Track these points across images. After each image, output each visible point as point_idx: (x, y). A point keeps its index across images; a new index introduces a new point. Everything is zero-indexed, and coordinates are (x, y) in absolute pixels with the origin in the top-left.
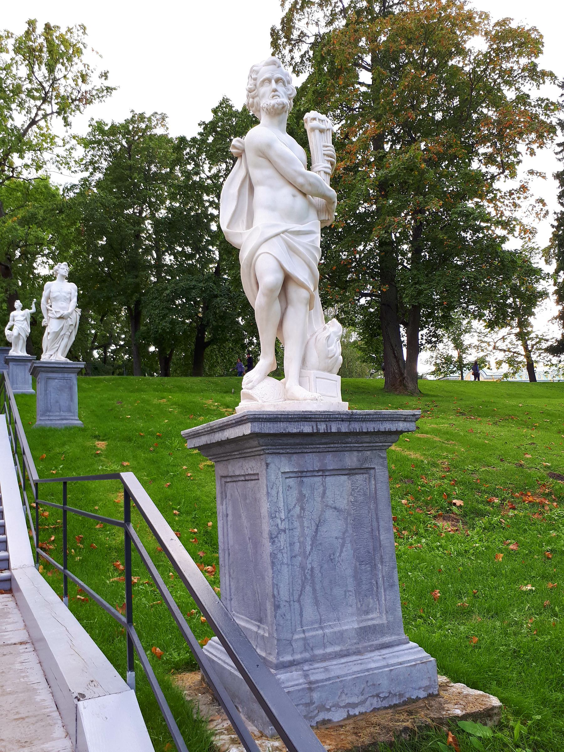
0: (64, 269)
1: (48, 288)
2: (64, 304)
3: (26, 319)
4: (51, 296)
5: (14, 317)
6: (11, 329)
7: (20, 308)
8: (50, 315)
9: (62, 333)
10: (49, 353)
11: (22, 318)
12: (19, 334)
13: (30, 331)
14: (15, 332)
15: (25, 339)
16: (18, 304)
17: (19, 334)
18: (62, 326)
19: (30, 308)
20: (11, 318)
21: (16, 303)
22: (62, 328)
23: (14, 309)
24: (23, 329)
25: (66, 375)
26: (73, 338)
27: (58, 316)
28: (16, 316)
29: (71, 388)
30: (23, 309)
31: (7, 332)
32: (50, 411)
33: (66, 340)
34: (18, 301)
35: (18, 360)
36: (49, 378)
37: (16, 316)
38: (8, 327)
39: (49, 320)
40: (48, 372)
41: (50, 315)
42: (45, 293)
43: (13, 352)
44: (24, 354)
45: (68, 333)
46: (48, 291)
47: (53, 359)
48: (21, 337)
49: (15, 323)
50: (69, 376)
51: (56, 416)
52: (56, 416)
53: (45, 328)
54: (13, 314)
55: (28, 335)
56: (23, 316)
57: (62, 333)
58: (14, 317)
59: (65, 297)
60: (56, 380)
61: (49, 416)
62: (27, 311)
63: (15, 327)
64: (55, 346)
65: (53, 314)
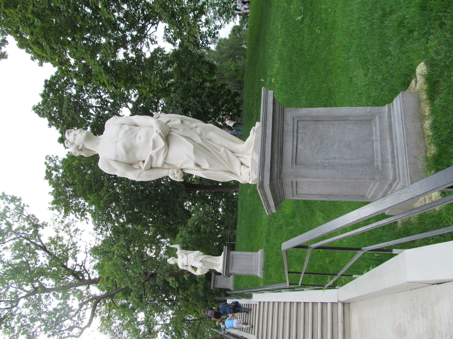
0: (75, 135)
1: (110, 165)
2: (141, 133)
3: (186, 254)
4: (125, 159)
5: (183, 265)
6: (194, 268)
7: (176, 259)
8: (159, 162)
9: (198, 140)
10: (237, 168)
11: (185, 257)
12: (201, 261)
13: (198, 252)
14: (198, 264)
15: (206, 256)
17: (201, 261)
18: (184, 140)
19: (177, 250)
20: (185, 268)
21: (170, 263)
22: (188, 138)
23: (176, 265)
24: (195, 257)
25: (289, 127)
27: (161, 143)
28: (183, 263)
29: (317, 120)
30: (177, 257)
32: (373, 161)
33: (212, 135)
35: (227, 264)
36: (295, 160)
37: (183, 263)
38: (193, 272)
39: (171, 166)
40: (281, 163)
41: (159, 162)
42: (120, 172)
43: (219, 269)
46: (114, 165)
48: (204, 260)
49: (190, 265)
50: (290, 122)
51: (383, 148)
52: (383, 148)
53: (187, 176)
55: (202, 253)
56: (183, 257)
57: (198, 140)
58: (183, 265)
59: (126, 132)
60: (300, 147)
61: (384, 162)
62: (179, 252)
63: (193, 265)
64: (224, 155)
65: (158, 154)
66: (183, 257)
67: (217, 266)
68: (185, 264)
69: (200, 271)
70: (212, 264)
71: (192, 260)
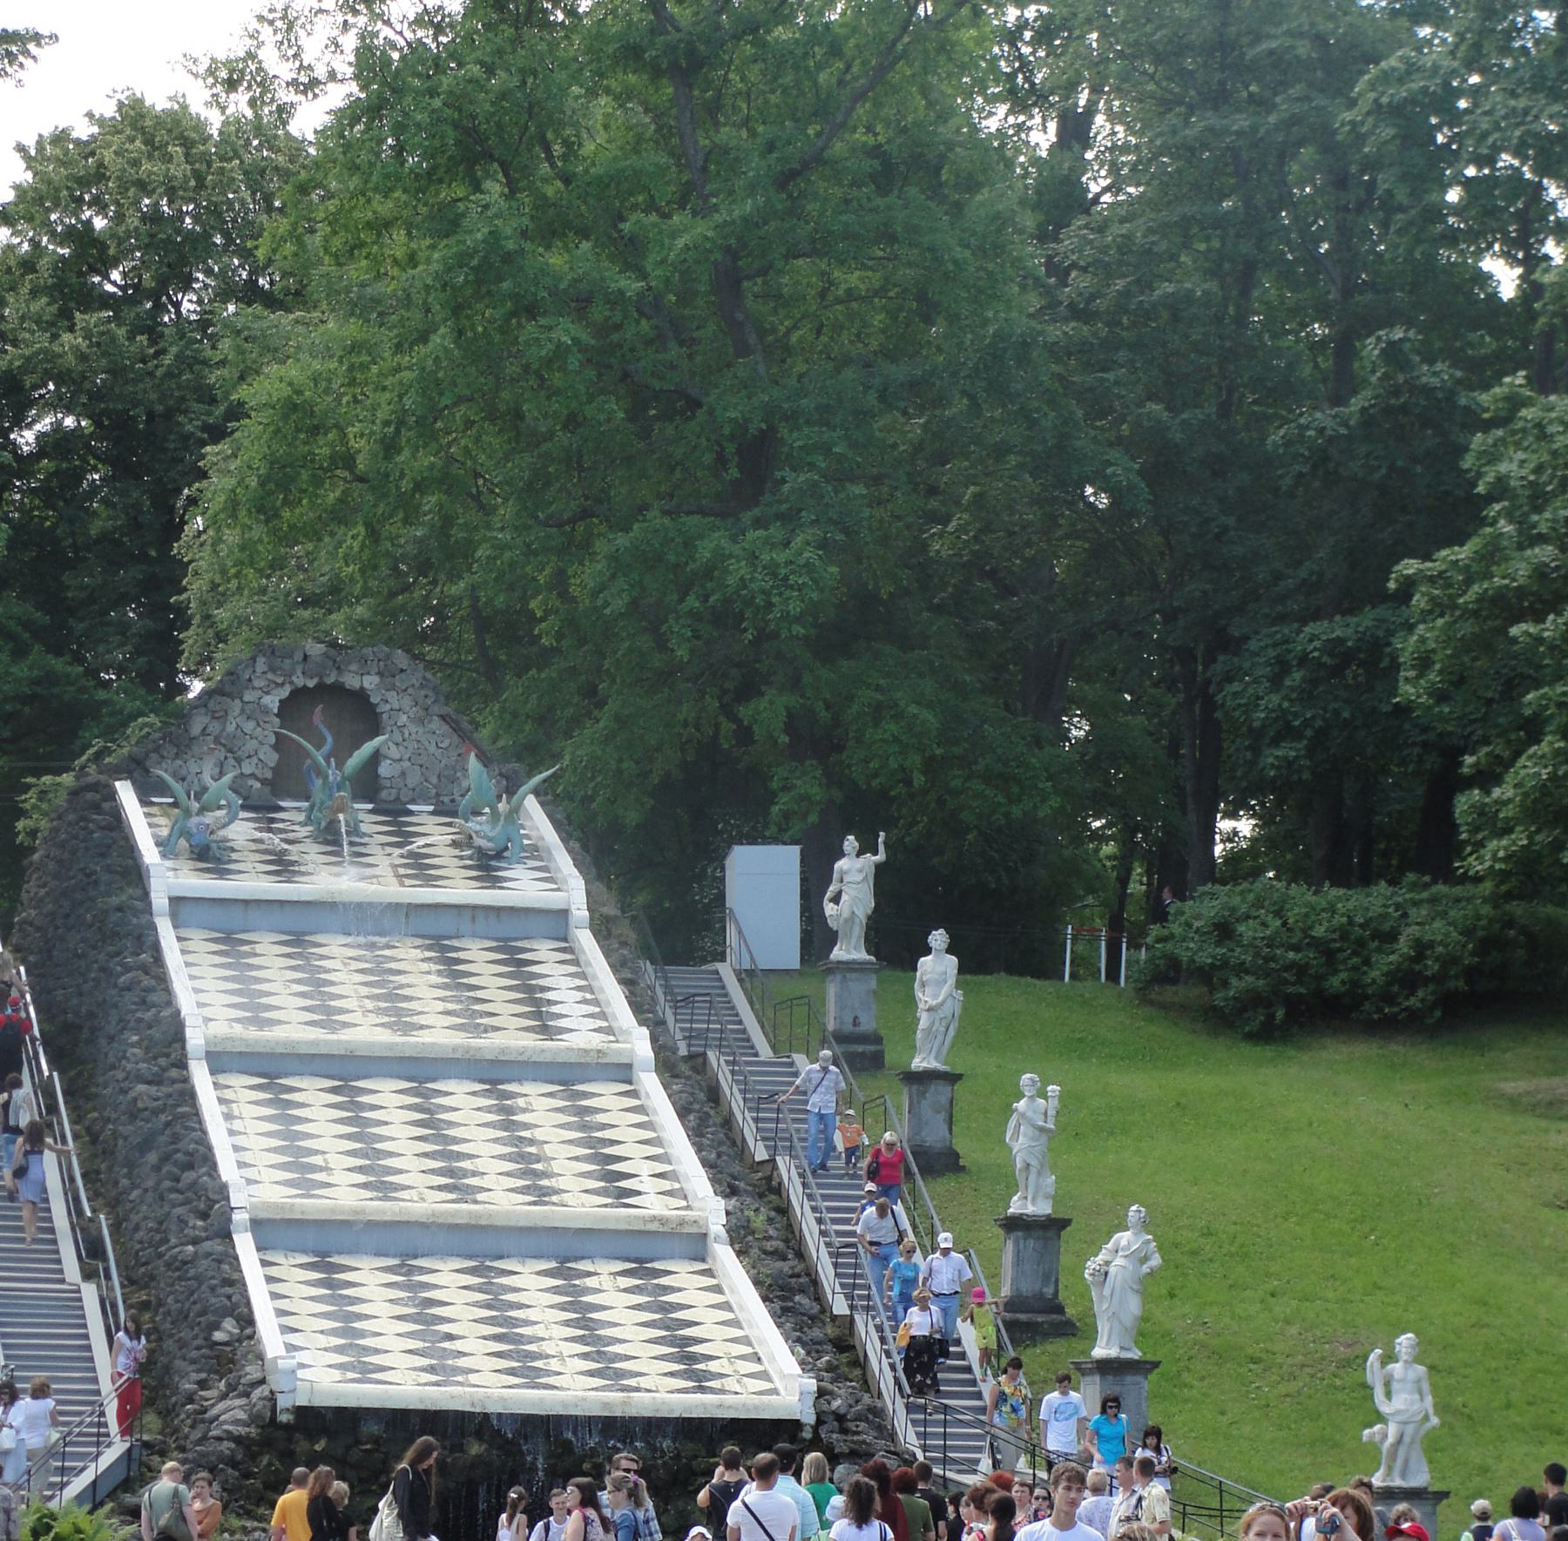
6: (836, 899)
11: (860, 877)
16: (850, 843)
19: (875, 853)
23: (842, 855)
26: (952, 1032)
30: (858, 856)
31: (830, 909)
34: (851, 838)
38: (828, 895)
44: (862, 955)
54: (841, 864)
56: (860, 871)
58: (842, 873)
62: (870, 860)
63: (844, 897)
69: (834, 913)
71: (853, 893)
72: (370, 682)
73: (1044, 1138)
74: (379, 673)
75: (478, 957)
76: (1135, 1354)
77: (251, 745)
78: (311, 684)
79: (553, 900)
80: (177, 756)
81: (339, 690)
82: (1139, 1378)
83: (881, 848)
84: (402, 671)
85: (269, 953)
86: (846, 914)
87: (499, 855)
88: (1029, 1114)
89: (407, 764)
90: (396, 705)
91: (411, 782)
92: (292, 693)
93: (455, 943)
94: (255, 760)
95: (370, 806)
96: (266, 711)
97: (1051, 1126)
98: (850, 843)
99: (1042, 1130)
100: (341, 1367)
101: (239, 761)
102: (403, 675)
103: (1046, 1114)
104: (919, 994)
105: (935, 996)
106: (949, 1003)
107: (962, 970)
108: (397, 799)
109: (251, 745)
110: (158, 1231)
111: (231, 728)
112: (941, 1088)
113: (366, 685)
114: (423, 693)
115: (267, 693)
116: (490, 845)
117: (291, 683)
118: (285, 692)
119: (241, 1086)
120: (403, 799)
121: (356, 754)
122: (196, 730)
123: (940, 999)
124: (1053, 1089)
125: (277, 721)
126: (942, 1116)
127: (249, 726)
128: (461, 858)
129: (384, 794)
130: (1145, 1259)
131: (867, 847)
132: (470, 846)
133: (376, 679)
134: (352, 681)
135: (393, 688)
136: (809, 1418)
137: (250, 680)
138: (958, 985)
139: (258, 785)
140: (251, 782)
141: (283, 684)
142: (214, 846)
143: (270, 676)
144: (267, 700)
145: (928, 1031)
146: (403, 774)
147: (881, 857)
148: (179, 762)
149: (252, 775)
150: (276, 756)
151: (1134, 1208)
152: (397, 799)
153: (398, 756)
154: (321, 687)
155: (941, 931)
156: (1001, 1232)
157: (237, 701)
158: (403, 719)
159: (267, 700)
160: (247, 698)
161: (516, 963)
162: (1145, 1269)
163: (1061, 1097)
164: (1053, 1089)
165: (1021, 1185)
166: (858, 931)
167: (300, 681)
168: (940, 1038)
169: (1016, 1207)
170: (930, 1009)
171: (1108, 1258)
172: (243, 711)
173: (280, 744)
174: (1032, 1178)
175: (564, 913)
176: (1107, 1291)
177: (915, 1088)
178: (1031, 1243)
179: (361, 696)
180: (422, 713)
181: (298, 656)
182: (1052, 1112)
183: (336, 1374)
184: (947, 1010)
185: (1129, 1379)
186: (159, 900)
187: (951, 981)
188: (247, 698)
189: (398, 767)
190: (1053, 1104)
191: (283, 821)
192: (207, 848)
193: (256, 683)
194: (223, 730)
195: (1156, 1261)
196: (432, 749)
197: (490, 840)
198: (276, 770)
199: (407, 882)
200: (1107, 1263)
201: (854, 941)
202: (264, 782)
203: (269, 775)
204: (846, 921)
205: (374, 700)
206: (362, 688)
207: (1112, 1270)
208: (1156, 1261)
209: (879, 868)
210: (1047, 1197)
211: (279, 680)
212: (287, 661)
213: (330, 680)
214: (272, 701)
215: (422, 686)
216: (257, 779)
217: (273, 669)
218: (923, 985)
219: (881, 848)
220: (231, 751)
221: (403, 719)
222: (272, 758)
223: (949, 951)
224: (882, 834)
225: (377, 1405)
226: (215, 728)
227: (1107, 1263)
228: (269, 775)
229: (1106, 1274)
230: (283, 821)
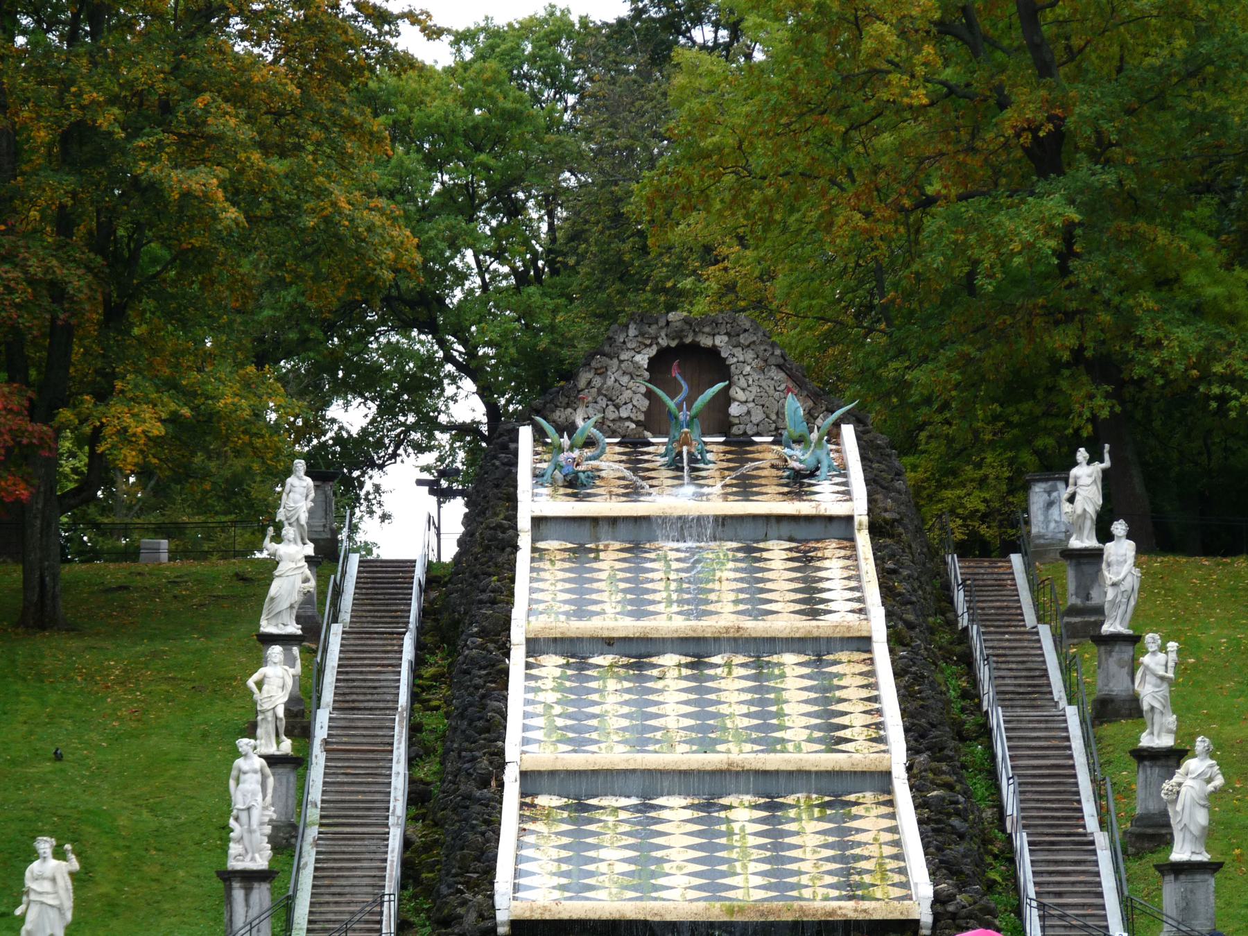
3: (1095, 481)
5: (1076, 478)
6: (1071, 499)
11: (1089, 481)
13: (1101, 502)
15: (1094, 517)
16: (1082, 454)
19: (1102, 461)
23: (1075, 464)
26: (1132, 603)
30: (1089, 463)
45: (1124, 600)
47: (1112, 629)
54: (1075, 472)
56: (1090, 476)
58: (1076, 478)
62: (1098, 467)
63: (1078, 498)
66: (1090, 476)
67: (1080, 538)
68: (1080, 482)
70: (1081, 529)
72: (720, 341)
73: (1165, 686)
74: (727, 334)
75: (777, 553)
76: (1204, 857)
77: (627, 394)
78: (673, 344)
79: (840, 509)
80: (568, 405)
81: (695, 347)
82: (1207, 877)
83: (1107, 457)
84: (746, 331)
85: (610, 560)
86: (1079, 511)
87: (812, 474)
88: (1152, 666)
89: (751, 405)
90: (740, 359)
91: (756, 419)
92: (658, 351)
93: (761, 545)
94: (630, 406)
95: (722, 439)
96: (637, 366)
97: (1171, 674)
98: (1082, 454)
99: (1162, 678)
100: (562, 888)
101: (617, 407)
102: (746, 335)
103: (1166, 665)
104: (1106, 573)
105: (1118, 574)
106: (1129, 579)
107: (1139, 551)
108: (745, 433)
109: (627, 394)
110: (454, 783)
111: (610, 382)
112: (1124, 648)
113: (717, 342)
114: (762, 348)
115: (639, 353)
116: (802, 466)
117: (658, 344)
118: (653, 351)
119: (551, 664)
120: (750, 433)
121: (700, 398)
122: (582, 383)
123: (1121, 577)
124: (1172, 646)
125: (647, 374)
126: (1126, 670)
127: (625, 380)
128: (781, 478)
129: (734, 430)
130: (1209, 781)
131: (1095, 457)
132: (786, 468)
133: (726, 338)
134: (706, 341)
135: (738, 345)
136: (926, 917)
137: (624, 342)
138: (1136, 565)
139: (633, 426)
140: (627, 424)
141: (651, 345)
142: (581, 475)
143: (640, 339)
144: (638, 358)
145: (1113, 602)
146: (749, 413)
147: (1107, 463)
148: (570, 410)
149: (629, 419)
150: (647, 403)
151: (1199, 739)
152: (745, 433)
153: (744, 399)
154: (681, 346)
155: (1121, 521)
156: (1134, 764)
157: (615, 361)
158: (748, 369)
159: (638, 358)
160: (622, 357)
161: (805, 560)
162: (1210, 787)
163: (1179, 652)
164: (1172, 646)
165: (1149, 724)
166: (1089, 525)
167: (664, 342)
168: (1123, 607)
169: (1146, 741)
170: (1114, 585)
171: (1180, 780)
172: (619, 367)
173: (649, 394)
174: (1157, 717)
175: (849, 519)
176: (1179, 808)
177: (1102, 648)
178: (1157, 770)
179: (714, 352)
180: (762, 363)
181: (662, 322)
182: (1171, 664)
183: (557, 894)
184: (1126, 585)
185: (1198, 877)
186: (524, 523)
187: (1131, 561)
188: (622, 357)
189: (744, 409)
190: (1173, 656)
191: (649, 453)
192: (576, 477)
193: (629, 345)
194: (605, 383)
195: (1219, 781)
196: (771, 391)
197: (801, 462)
198: (648, 413)
199: (731, 498)
200: (1180, 785)
201: (1086, 532)
202: (638, 423)
203: (642, 417)
204: (1079, 516)
205: (724, 355)
206: (714, 346)
207: (1183, 790)
208: (1219, 781)
209: (1104, 471)
210: (1169, 731)
211: (648, 342)
212: (654, 327)
213: (688, 340)
214: (643, 359)
215: (762, 343)
216: (632, 421)
217: (642, 334)
218: (1109, 565)
219: (1107, 457)
220: (610, 400)
221: (748, 369)
222: (644, 404)
223: (1129, 537)
224: (1107, 446)
225: (583, 916)
226: (597, 381)
227: (1180, 785)
228: (642, 417)
229: (1178, 792)
230: (649, 453)
